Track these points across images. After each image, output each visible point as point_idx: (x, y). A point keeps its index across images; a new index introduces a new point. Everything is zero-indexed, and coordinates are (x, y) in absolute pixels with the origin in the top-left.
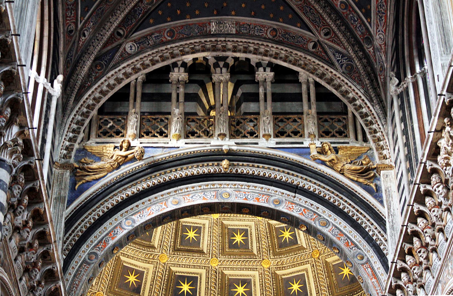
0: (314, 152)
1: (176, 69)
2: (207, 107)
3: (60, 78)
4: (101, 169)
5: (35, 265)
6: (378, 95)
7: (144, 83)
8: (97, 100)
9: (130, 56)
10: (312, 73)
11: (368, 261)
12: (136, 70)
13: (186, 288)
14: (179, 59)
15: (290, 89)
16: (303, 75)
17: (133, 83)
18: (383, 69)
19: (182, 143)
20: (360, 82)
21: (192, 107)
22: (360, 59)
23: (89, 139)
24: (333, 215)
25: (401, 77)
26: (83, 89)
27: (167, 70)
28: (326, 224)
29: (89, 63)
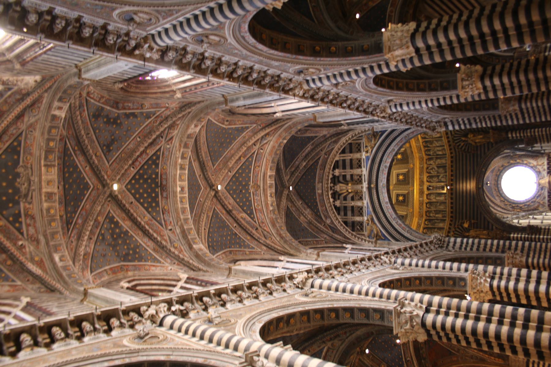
0: (368, 154)
3: (344, 245)
5: (420, 251)
6: (345, 132)
8: (349, 232)
9: (332, 221)
11: (408, 135)
12: (337, 219)
13: (401, 198)
14: (332, 203)
15: (341, 163)
16: (337, 158)
18: (336, 131)
19: (365, 202)
20: (340, 139)
22: (332, 139)
23: (364, 235)
25: (341, 125)
26: (345, 237)
27: (336, 207)
28: (393, 150)
29: (336, 236)
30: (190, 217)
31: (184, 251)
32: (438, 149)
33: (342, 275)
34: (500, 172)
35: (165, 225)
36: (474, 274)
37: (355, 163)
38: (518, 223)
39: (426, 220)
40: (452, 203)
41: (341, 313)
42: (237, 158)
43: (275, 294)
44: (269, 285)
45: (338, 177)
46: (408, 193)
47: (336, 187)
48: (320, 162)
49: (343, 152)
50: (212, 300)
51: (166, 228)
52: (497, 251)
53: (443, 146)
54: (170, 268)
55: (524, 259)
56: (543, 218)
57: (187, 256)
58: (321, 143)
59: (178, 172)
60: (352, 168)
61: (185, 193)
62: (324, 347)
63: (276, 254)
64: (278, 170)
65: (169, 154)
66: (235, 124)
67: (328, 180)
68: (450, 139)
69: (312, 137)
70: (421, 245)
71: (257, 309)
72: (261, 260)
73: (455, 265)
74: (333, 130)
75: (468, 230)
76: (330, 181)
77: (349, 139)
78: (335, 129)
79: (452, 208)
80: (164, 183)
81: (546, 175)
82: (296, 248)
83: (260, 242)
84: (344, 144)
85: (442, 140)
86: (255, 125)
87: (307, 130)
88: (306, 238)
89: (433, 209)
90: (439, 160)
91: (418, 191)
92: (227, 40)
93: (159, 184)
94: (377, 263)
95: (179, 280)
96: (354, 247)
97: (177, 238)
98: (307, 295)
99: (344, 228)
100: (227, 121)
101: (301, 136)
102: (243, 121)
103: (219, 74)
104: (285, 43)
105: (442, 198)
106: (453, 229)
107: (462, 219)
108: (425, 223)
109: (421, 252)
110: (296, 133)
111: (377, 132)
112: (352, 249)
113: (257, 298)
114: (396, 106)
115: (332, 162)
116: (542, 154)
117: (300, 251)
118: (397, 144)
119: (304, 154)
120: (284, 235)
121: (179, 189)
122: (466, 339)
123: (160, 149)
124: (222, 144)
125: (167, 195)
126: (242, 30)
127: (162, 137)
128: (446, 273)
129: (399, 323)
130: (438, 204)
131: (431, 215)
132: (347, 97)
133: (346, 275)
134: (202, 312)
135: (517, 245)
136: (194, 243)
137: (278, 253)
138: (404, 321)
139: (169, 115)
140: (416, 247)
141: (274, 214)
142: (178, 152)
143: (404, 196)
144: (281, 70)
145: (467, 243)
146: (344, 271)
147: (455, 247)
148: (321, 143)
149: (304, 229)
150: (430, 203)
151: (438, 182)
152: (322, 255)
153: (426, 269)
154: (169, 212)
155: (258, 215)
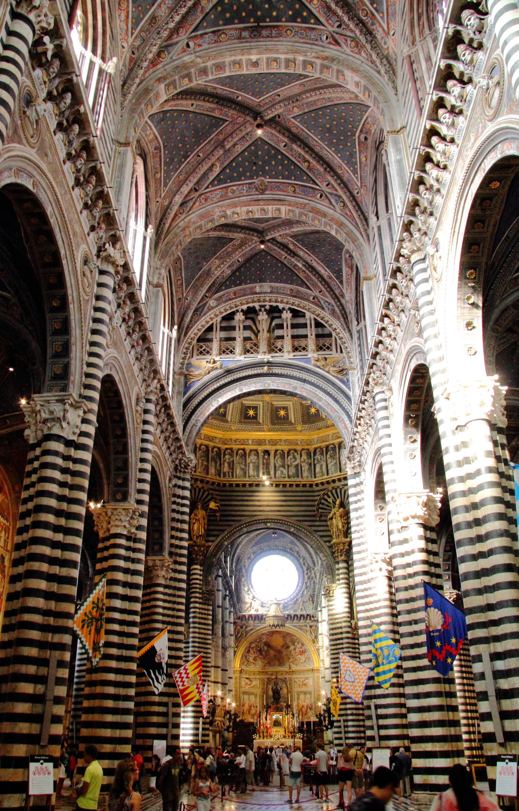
4: (200, 375)
6: (348, 327)
7: (221, 322)
8: (196, 334)
9: (213, 308)
11: (343, 420)
12: (216, 316)
13: (251, 413)
14: (240, 308)
15: (301, 321)
16: (308, 315)
18: (350, 313)
19: (242, 358)
20: (339, 319)
21: (248, 334)
24: (325, 395)
26: (188, 328)
27: (233, 313)
28: (321, 399)
29: (190, 315)
30: (210, 77)
31: (155, 69)
32: (324, 466)
33: (124, 320)
35: (195, 36)
36: (134, 512)
37: (302, 343)
38: (218, 576)
39: (219, 449)
40: (244, 485)
41: (61, 315)
42: (307, 157)
43: (85, 212)
44: (100, 203)
45: (280, 317)
46: (259, 423)
48: (303, 289)
50: (68, 108)
51: (189, 38)
52: (172, 545)
53: (328, 474)
54: (125, 45)
55: (161, 581)
56: (227, 609)
57: (147, 75)
58: (331, 290)
59: (283, 57)
60: (294, 337)
61: (247, 69)
62: (9, 292)
63: (159, 219)
65: (313, 39)
66: (360, 151)
67: (276, 301)
68: (337, 484)
70: (177, 439)
71: (57, 183)
72: (147, 197)
73: (147, 487)
74: (351, 308)
75: (205, 507)
76: (274, 304)
78: (353, 311)
79: (238, 485)
80: (264, 33)
81: (287, 612)
82: (167, 252)
83: (175, 195)
84: (331, 326)
85: (336, 471)
86: (359, 184)
87: (351, 268)
88: (186, 268)
89: (236, 459)
90: (307, 467)
91: (262, 438)
92: (490, 121)
93: (261, 24)
94: (146, 372)
95: (103, 59)
96: (173, 342)
97: (174, 58)
98: (86, 262)
100: (366, 139)
102: (366, 165)
103: (437, 113)
104: (483, 222)
105: (252, 472)
106: (206, 488)
107: (221, 500)
108: (214, 447)
109: (166, 440)
110: (348, 251)
111: (347, 374)
112: (170, 339)
113: (78, 183)
114: (385, 400)
116: (316, 608)
117: (163, 257)
118: (329, 404)
119: (315, 264)
121: (254, 58)
122: (30, 498)
123: (320, 23)
124: (329, 130)
125: (244, 38)
126: (506, 145)
127: (339, 26)
128: (134, 474)
129: (48, 402)
131: (227, 457)
132: (399, 325)
133: (124, 326)
134: (46, 91)
135: (181, 572)
136: (168, 86)
137: (160, 224)
138: (52, 409)
139: (376, 37)
140: (174, 431)
142: (314, 54)
143: (255, 417)
144: (440, 216)
145: (183, 505)
146: (131, 323)
147: (176, 489)
148: (332, 290)
149: (198, 266)
151: (275, 467)
152: (159, 291)
153: (139, 445)
154: (216, 42)
155: (218, 192)
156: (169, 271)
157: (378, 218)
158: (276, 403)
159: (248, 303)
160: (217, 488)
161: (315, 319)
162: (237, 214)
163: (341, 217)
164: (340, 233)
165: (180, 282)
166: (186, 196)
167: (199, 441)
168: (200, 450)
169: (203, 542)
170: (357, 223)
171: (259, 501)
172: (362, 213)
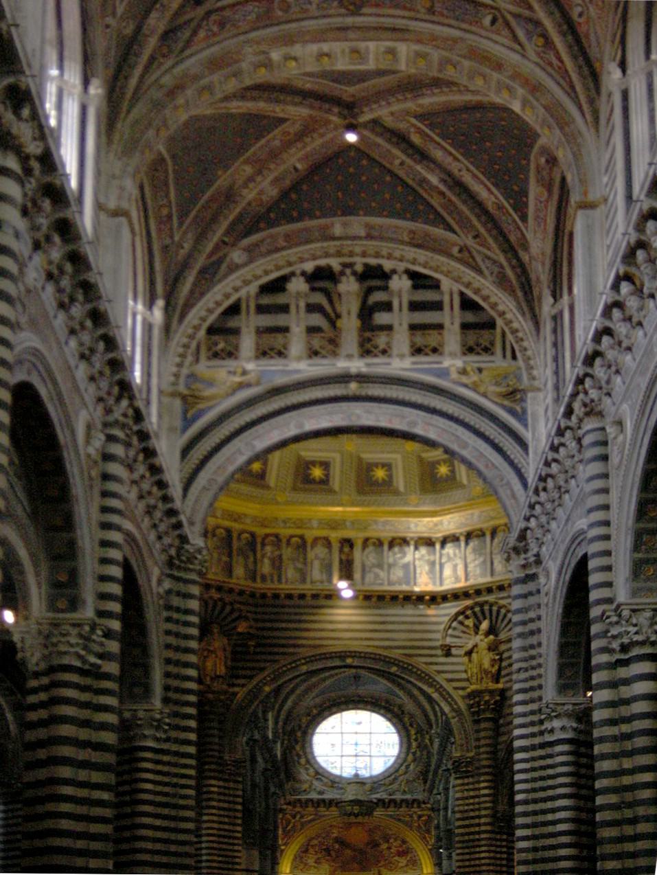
1: (294, 279)
2: (333, 315)
6: (532, 309)
7: (258, 295)
10: (456, 281)
12: (247, 283)
14: (298, 268)
16: (446, 284)
17: (244, 297)
20: (512, 292)
21: (317, 320)
22: (513, 267)
27: (284, 279)
34: (385, 708)
37: (432, 339)
40: (302, 596)
45: (386, 288)
47: (352, 279)
49: (468, 304)
60: (413, 328)
64: (413, 86)
69: (526, 204)
74: (541, 272)
77: (508, 323)
81: (378, 796)
89: (287, 552)
90: (427, 568)
99: (218, 304)
101: (533, 166)
105: (316, 573)
107: (256, 620)
108: (243, 532)
115: (436, 270)
120: (180, 101)
130: (300, 566)
141: (257, 66)
150: (302, 545)
156: (141, 188)
157: (624, 71)
158: (368, 457)
159: (314, 258)
160: (251, 601)
161: (462, 294)
162: (295, 59)
163: (538, 70)
164: (533, 108)
165: (165, 212)
166: (177, 14)
167: (212, 521)
168: (214, 535)
169: (225, 687)
170: (573, 87)
171: (331, 622)
172: (589, 62)
